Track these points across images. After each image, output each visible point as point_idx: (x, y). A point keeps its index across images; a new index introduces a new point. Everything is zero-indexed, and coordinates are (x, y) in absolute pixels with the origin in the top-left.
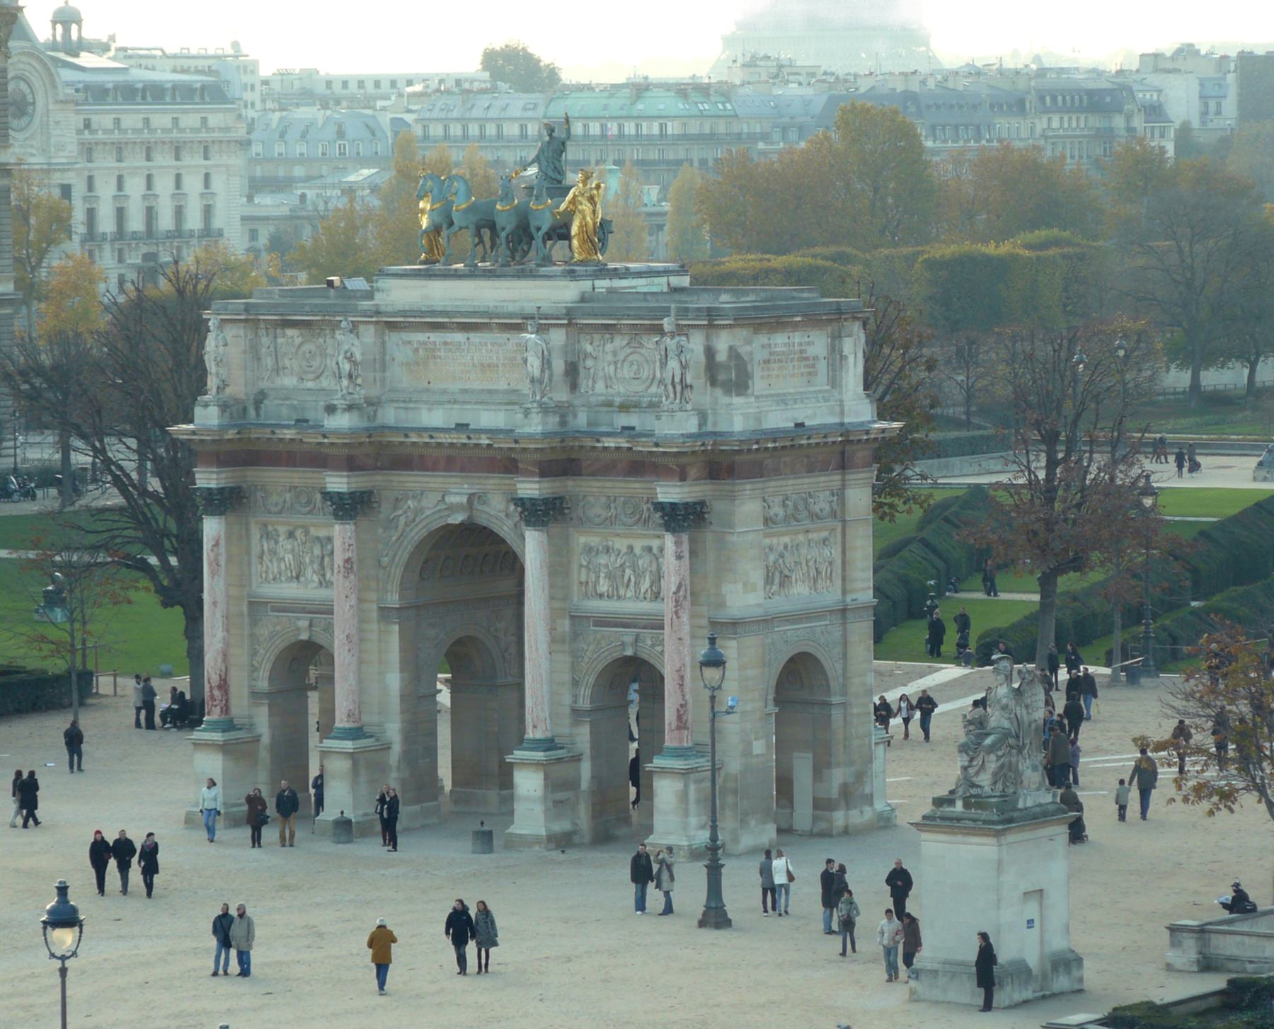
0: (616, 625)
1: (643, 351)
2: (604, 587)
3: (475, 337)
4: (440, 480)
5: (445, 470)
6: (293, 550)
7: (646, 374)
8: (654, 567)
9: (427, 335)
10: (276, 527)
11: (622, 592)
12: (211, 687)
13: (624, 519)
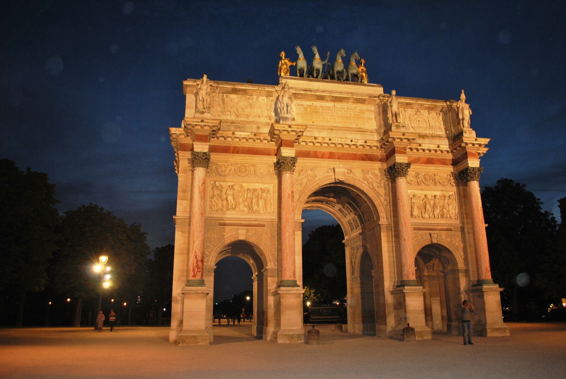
0: (425, 229)
1: (423, 117)
2: (416, 212)
3: (338, 105)
4: (327, 162)
5: (329, 158)
6: (233, 195)
7: (425, 126)
8: (441, 204)
9: (312, 102)
10: (221, 183)
11: (423, 215)
12: (197, 261)
13: (425, 182)
